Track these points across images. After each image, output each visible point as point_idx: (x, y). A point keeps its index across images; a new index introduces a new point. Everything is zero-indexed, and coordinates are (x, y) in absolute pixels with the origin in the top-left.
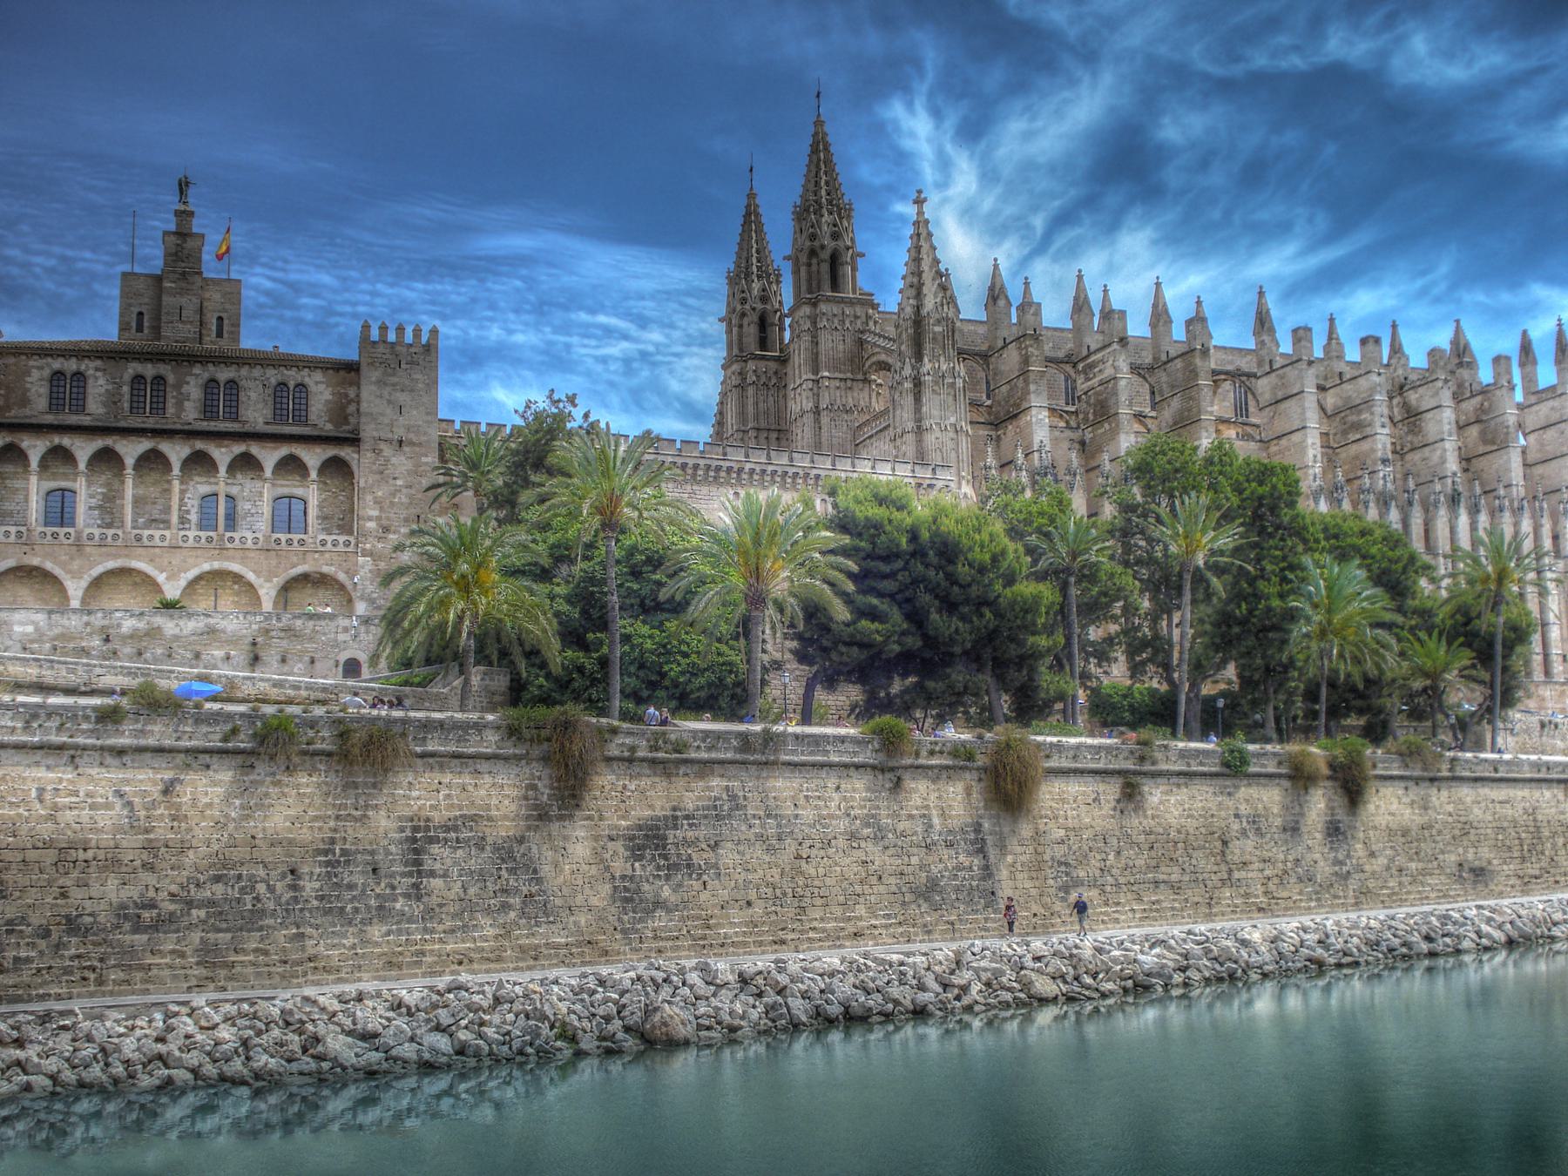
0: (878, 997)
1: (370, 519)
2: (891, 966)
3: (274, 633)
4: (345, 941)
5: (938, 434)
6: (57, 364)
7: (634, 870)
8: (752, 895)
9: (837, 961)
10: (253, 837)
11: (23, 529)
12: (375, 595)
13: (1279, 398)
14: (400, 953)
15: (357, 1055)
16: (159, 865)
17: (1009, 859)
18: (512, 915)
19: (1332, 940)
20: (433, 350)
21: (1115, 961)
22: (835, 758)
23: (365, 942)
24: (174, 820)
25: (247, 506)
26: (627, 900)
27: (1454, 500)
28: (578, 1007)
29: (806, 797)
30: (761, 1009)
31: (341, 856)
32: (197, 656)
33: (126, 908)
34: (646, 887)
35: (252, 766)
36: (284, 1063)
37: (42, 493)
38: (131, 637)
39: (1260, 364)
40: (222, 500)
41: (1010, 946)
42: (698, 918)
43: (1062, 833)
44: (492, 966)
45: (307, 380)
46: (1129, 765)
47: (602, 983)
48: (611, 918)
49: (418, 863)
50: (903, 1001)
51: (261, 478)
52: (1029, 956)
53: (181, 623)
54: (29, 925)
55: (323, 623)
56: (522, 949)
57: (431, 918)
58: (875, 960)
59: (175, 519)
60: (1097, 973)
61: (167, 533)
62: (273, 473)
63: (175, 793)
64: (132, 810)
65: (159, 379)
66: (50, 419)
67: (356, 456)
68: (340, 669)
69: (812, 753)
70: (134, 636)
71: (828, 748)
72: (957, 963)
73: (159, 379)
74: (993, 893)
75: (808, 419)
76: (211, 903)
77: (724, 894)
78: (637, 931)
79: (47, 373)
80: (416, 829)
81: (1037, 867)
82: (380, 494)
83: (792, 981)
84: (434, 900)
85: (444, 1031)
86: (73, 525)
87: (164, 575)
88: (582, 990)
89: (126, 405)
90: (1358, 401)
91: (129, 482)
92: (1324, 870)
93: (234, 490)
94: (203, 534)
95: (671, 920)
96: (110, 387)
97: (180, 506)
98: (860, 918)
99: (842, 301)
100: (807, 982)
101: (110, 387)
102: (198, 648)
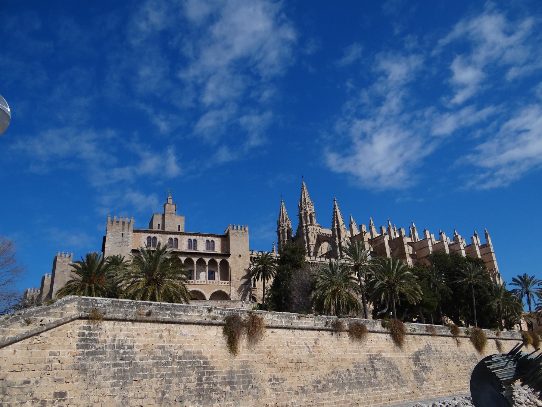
1: (234, 276)
4: (364, 393)
6: (149, 235)
12: (236, 297)
13: (422, 248)
16: (319, 368)
18: (396, 383)
22: (444, 333)
24: (319, 352)
31: (357, 364)
33: (314, 383)
34: (420, 374)
35: (332, 334)
49: (373, 366)
54: (293, 390)
55: (235, 303)
56: (401, 395)
69: (439, 332)
76: (332, 381)
79: (146, 237)
80: (370, 355)
90: (440, 248)
95: (427, 385)
99: (313, 225)
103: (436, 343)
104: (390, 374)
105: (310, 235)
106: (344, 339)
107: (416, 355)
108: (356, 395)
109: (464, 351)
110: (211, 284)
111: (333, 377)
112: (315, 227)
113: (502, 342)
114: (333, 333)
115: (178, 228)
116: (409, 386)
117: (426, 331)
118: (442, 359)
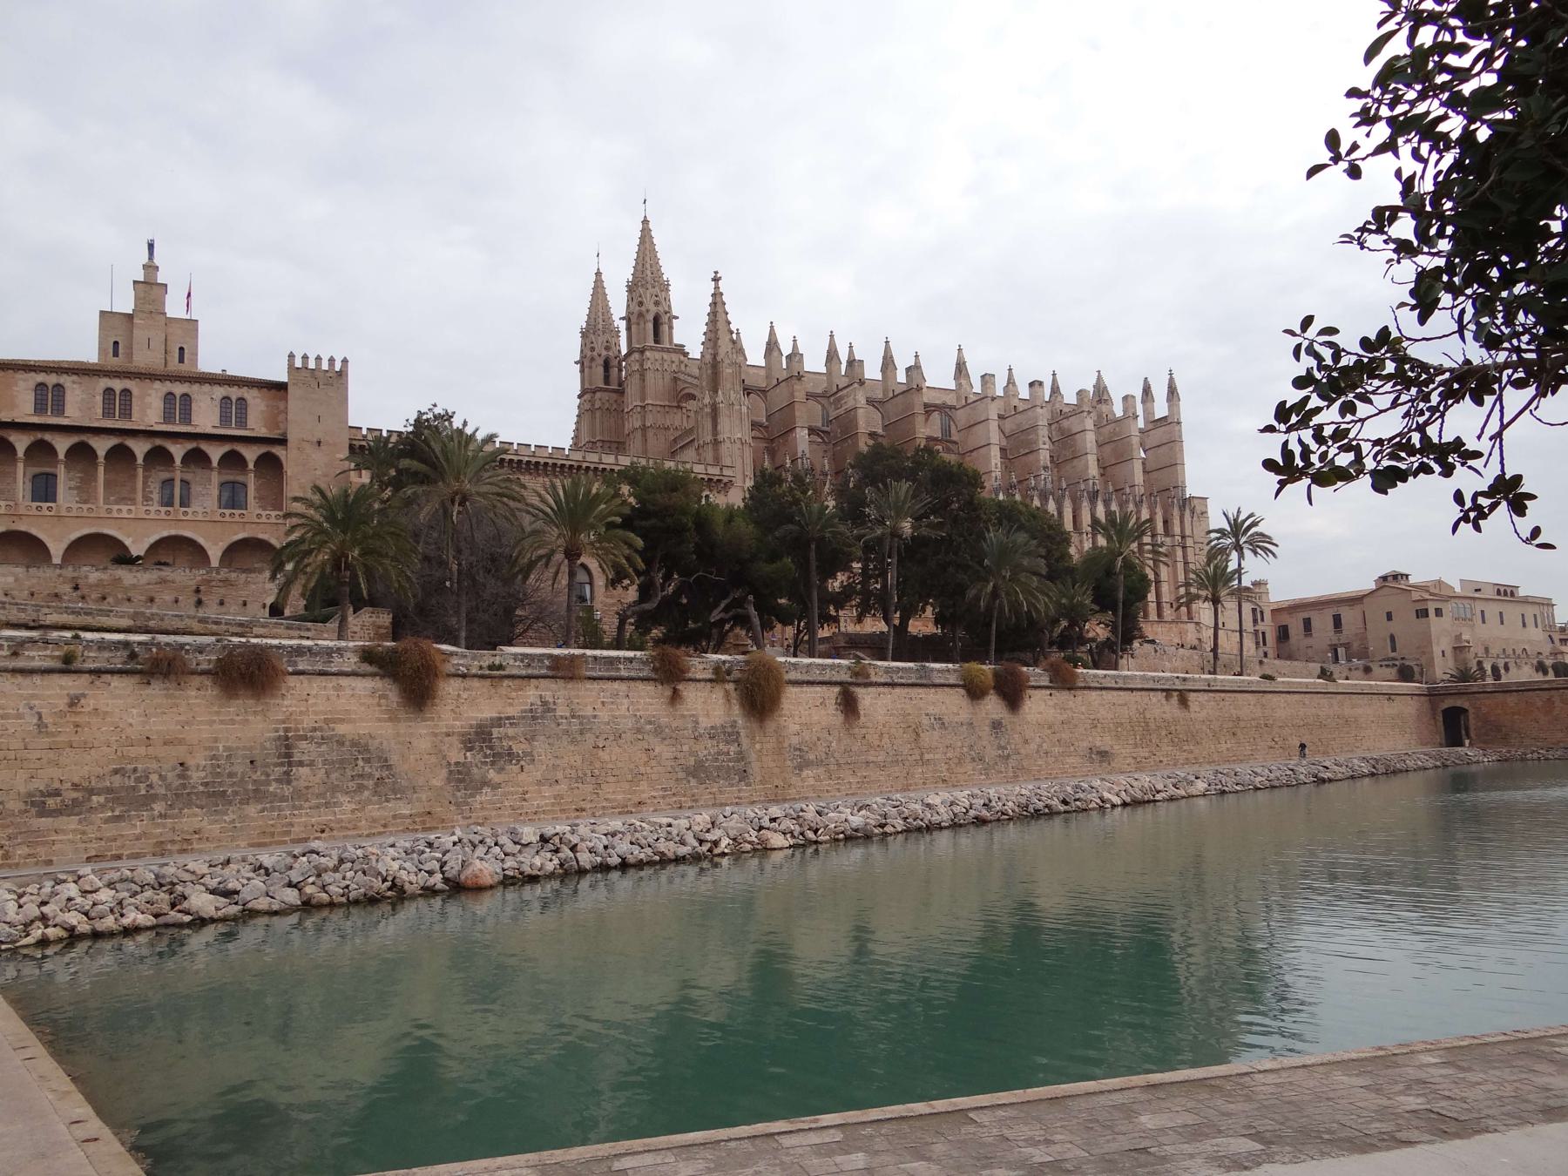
0: (649, 851)
2: (661, 827)
3: (214, 583)
4: (226, 818)
5: (730, 446)
6: (41, 378)
7: (466, 758)
8: (560, 775)
9: (620, 823)
10: (148, 738)
11: (12, 503)
14: (272, 825)
15: (217, 909)
17: (758, 746)
18: (366, 793)
19: (993, 804)
20: (344, 378)
21: (831, 820)
22: (624, 673)
23: (243, 818)
24: (77, 726)
25: (199, 488)
26: (461, 781)
27: (1093, 497)
28: (408, 865)
29: (603, 703)
30: (556, 861)
31: (224, 751)
32: (152, 600)
33: (34, 796)
34: (475, 770)
36: (152, 918)
37: (29, 476)
38: (97, 586)
39: (958, 399)
40: (177, 484)
41: (753, 811)
42: (517, 793)
43: (797, 727)
44: (350, 833)
45: (246, 396)
46: (846, 677)
47: (430, 845)
48: (446, 794)
49: (288, 755)
50: (666, 852)
51: (212, 469)
52: (767, 819)
53: (138, 575)
55: (253, 575)
56: (374, 821)
57: (299, 797)
58: (649, 823)
59: (139, 497)
60: (817, 830)
61: (132, 508)
62: (219, 464)
63: (79, 705)
64: (40, 718)
65: (126, 392)
66: (36, 420)
67: (284, 452)
68: (267, 610)
69: (607, 670)
70: (99, 584)
71: (622, 667)
72: (713, 823)
73: (126, 392)
74: (745, 771)
75: (639, 434)
76: (109, 790)
77: (538, 775)
78: (468, 804)
79: (32, 384)
80: (287, 730)
81: (779, 750)
82: (303, 481)
83: (582, 840)
84: (302, 784)
85: (295, 886)
86: (55, 501)
87: (131, 539)
88: (413, 851)
89: (100, 411)
91: (101, 469)
92: (991, 753)
93: (188, 477)
94: (163, 509)
96: (84, 396)
97: (144, 490)
98: (643, 792)
99: (663, 350)
100: (594, 840)
101: (84, 396)
102: (153, 594)
103: (578, 697)
104: (349, 773)
105: (650, 376)
106: (193, 693)
107: (480, 726)
108: (194, 819)
109: (693, 715)
110: (227, 519)
111: (117, 781)
112: (666, 356)
113: (860, 692)
114: (152, 681)
115: (177, 355)
116: (419, 800)
117: (549, 668)
118: (588, 735)
